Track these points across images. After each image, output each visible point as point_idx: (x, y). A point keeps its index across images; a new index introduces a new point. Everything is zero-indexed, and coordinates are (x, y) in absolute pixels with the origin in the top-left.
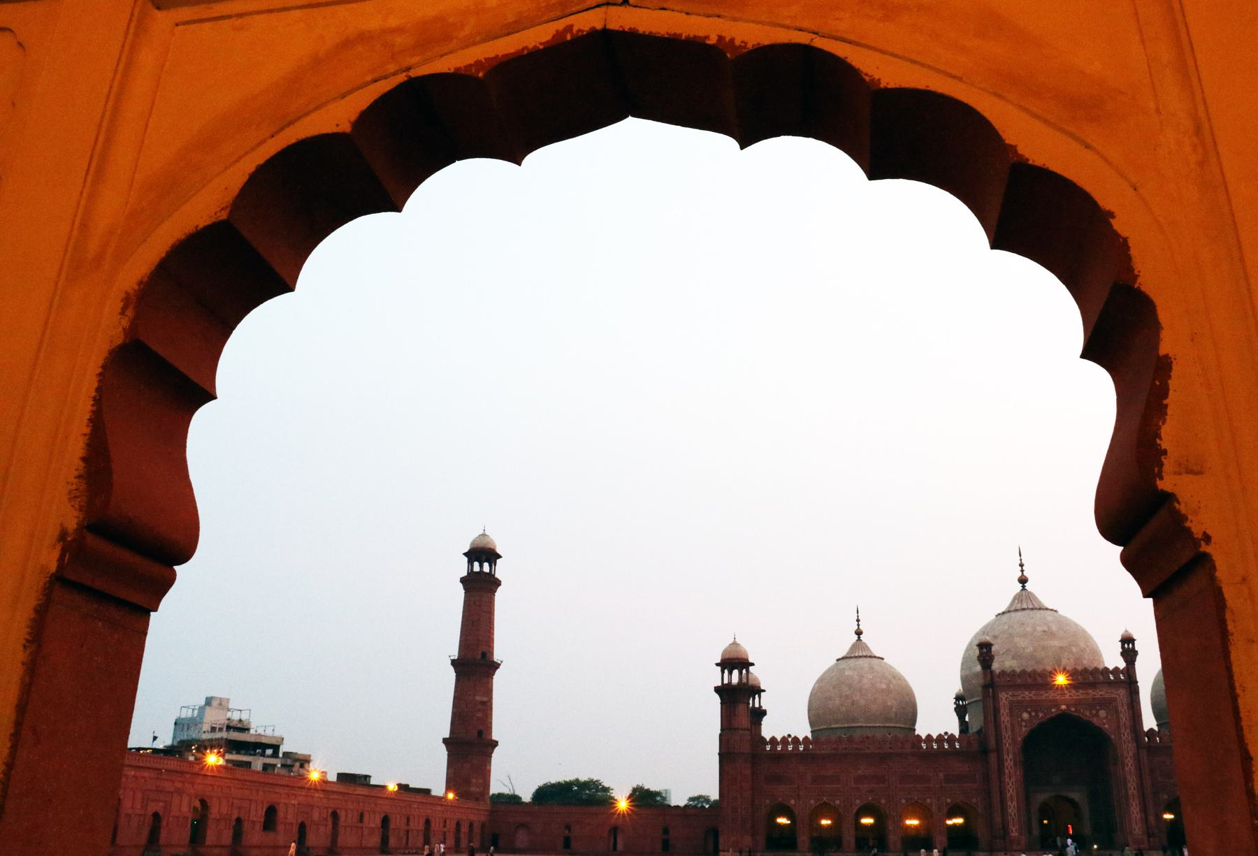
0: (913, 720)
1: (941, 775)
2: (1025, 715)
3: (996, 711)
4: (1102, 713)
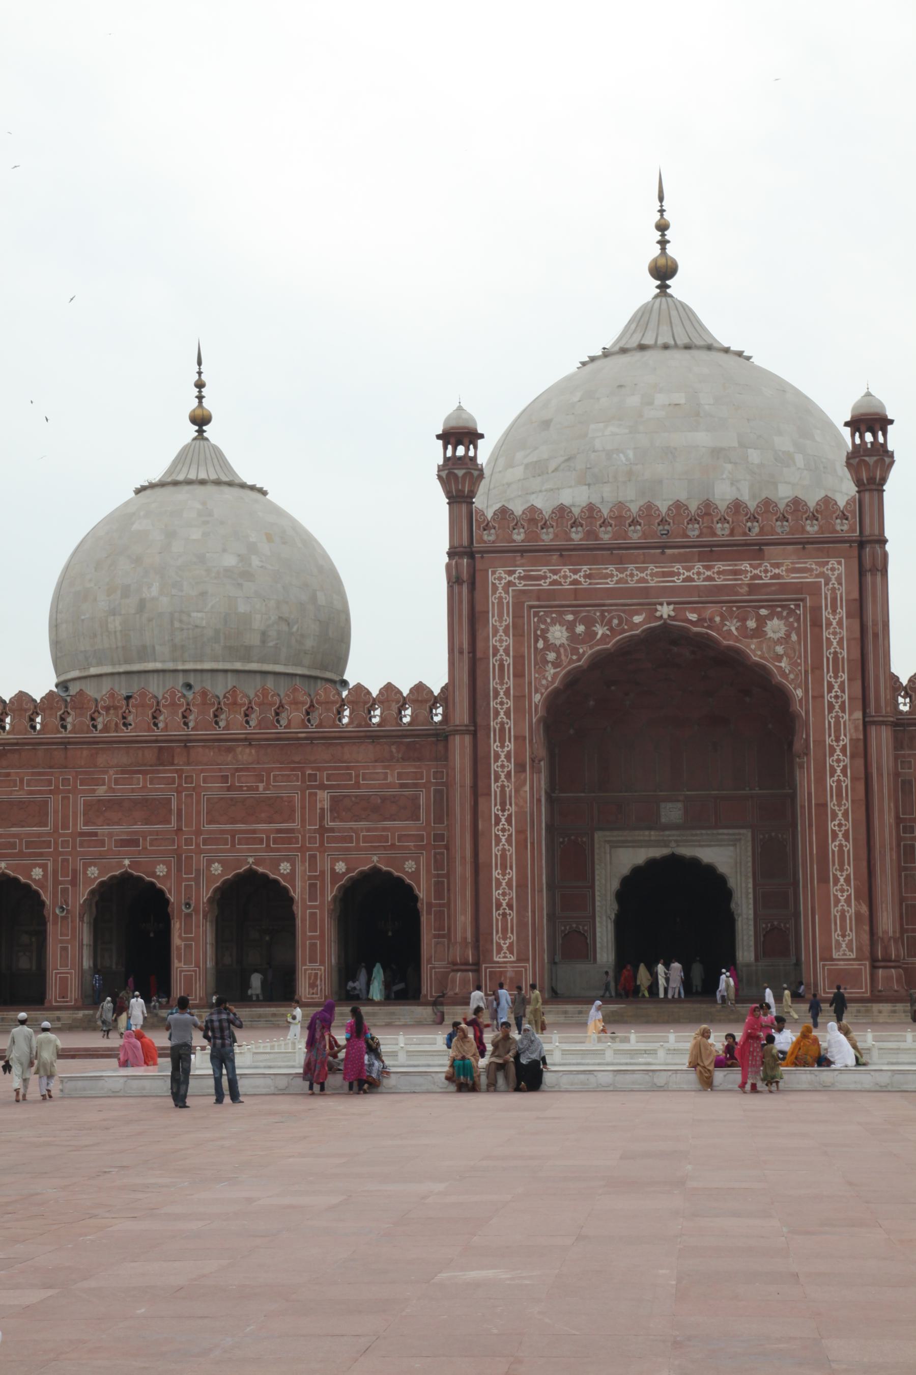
0: (340, 660)
1: (324, 798)
2: (558, 634)
4: (775, 628)
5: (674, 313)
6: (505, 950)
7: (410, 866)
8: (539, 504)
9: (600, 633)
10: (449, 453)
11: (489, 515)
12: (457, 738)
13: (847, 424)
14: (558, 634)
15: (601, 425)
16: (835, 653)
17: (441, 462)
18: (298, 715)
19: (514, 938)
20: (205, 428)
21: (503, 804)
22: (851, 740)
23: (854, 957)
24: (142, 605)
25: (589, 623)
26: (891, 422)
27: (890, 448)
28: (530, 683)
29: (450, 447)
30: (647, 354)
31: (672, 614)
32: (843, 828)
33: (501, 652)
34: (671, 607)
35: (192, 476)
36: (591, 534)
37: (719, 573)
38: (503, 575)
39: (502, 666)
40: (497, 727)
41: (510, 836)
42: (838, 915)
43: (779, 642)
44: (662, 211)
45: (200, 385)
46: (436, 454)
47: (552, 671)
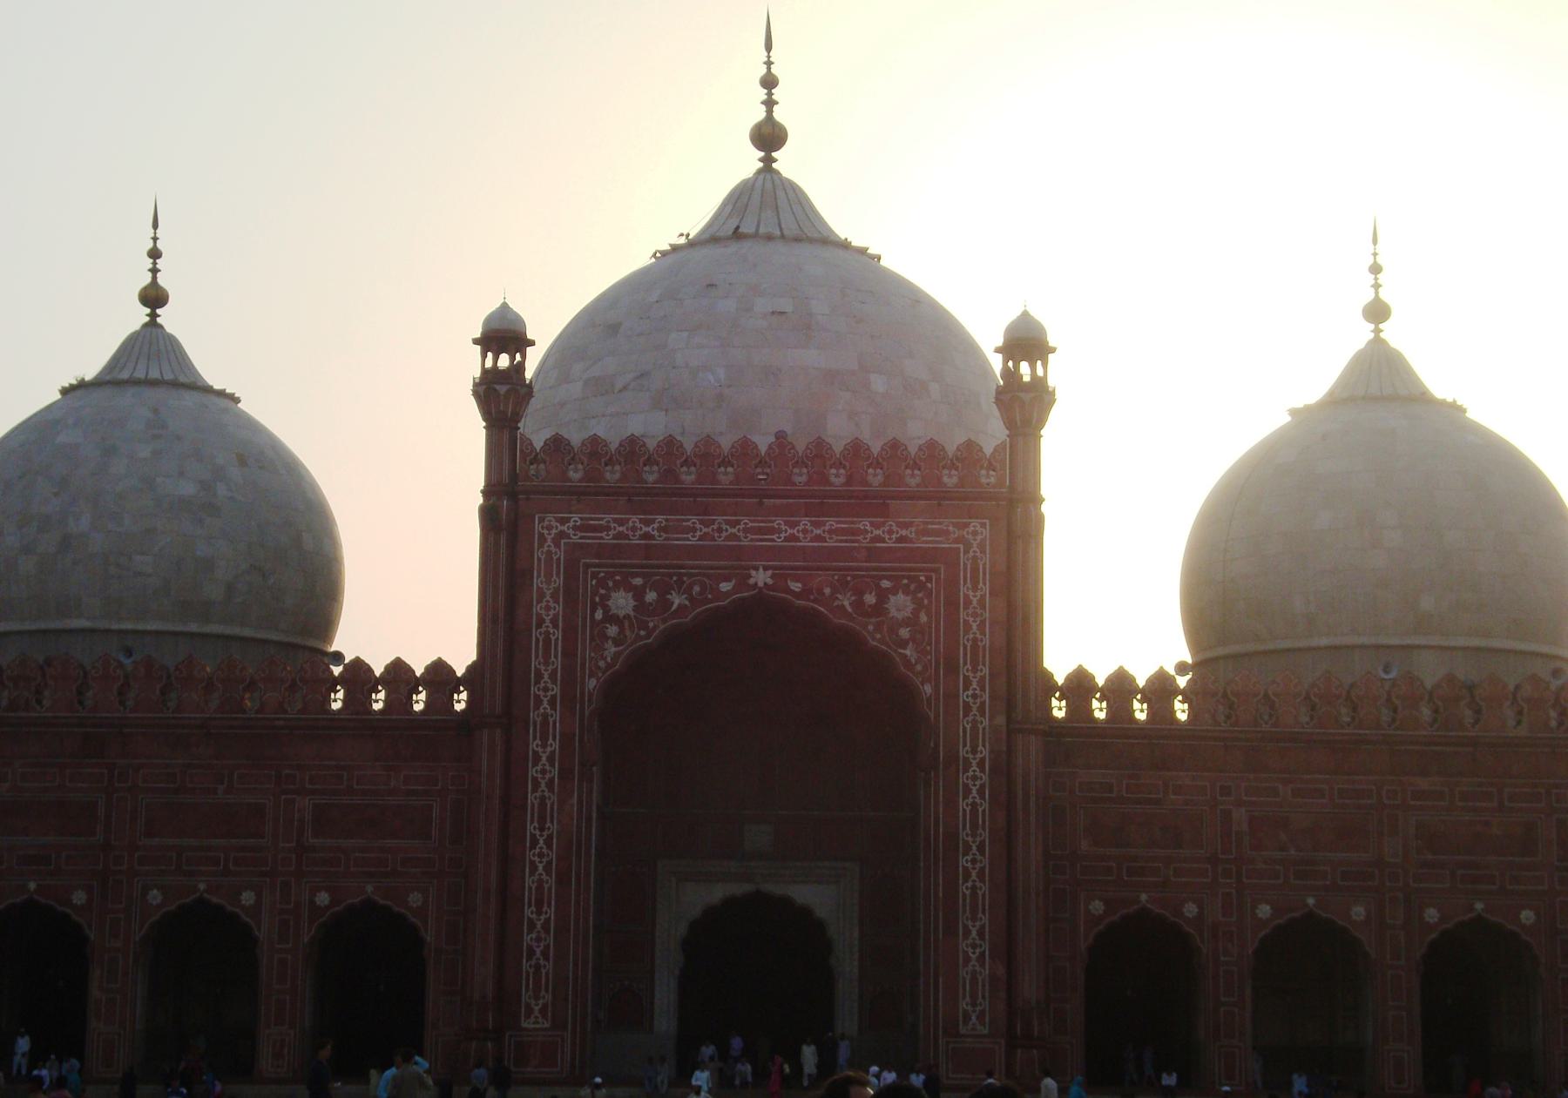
2: (622, 602)
5: (781, 194)
6: (536, 1013)
7: (415, 899)
8: (601, 432)
9: (677, 602)
10: (489, 363)
11: (538, 444)
13: (998, 350)
14: (622, 602)
15: (685, 334)
16: (975, 640)
17: (478, 374)
19: (549, 997)
20: (158, 311)
21: (542, 820)
22: (991, 752)
23: (986, 1032)
25: (663, 591)
26: (1053, 350)
27: (1051, 382)
28: (583, 665)
29: (490, 355)
30: (746, 246)
31: (770, 581)
32: (978, 865)
33: (548, 623)
34: (770, 572)
35: (140, 374)
36: (669, 474)
37: (830, 532)
38: (554, 524)
39: (547, 642)
40: (539, 720)
41: (550, 863)
42: (968, 978)
43: (906, 622)
44: (769, 63)
45: (155, 254)
46: (471, 363)
47: (613, 649)
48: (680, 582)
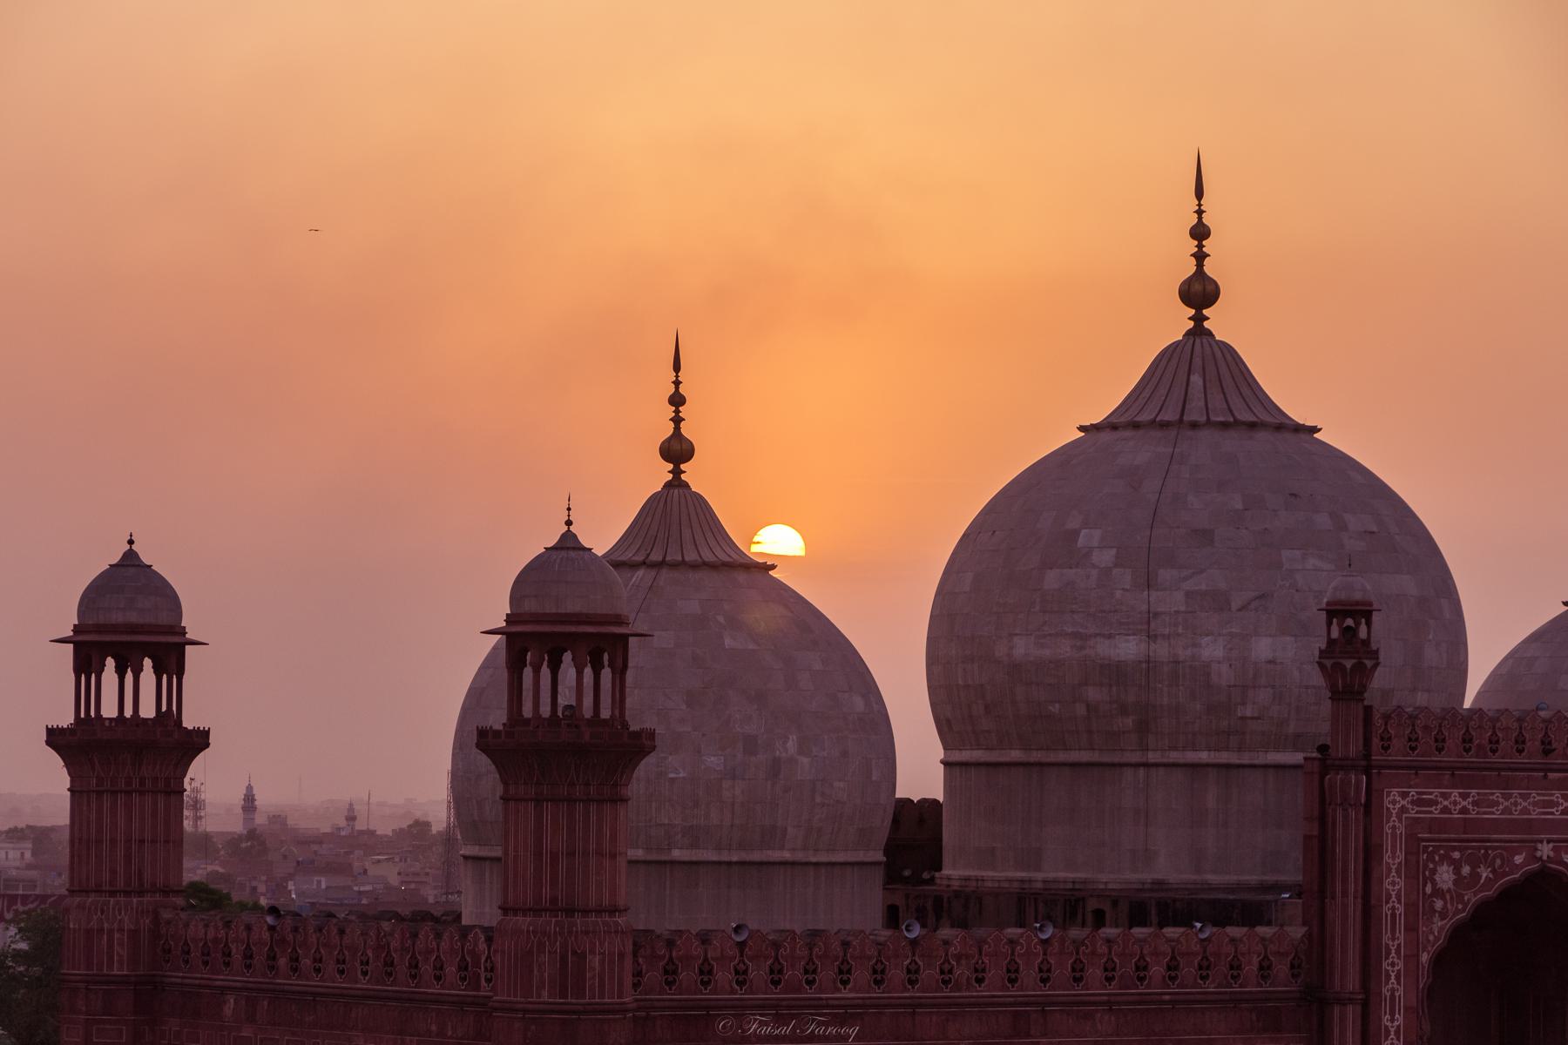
2: (1445, 876)
3: (1370, 854)
12: (1350, 1008)
18: (1157, 970)
20: (683, 467)
24: (775, 768)
31: (1552, 854)
45: (677, 400)
48: (1486, 855)
